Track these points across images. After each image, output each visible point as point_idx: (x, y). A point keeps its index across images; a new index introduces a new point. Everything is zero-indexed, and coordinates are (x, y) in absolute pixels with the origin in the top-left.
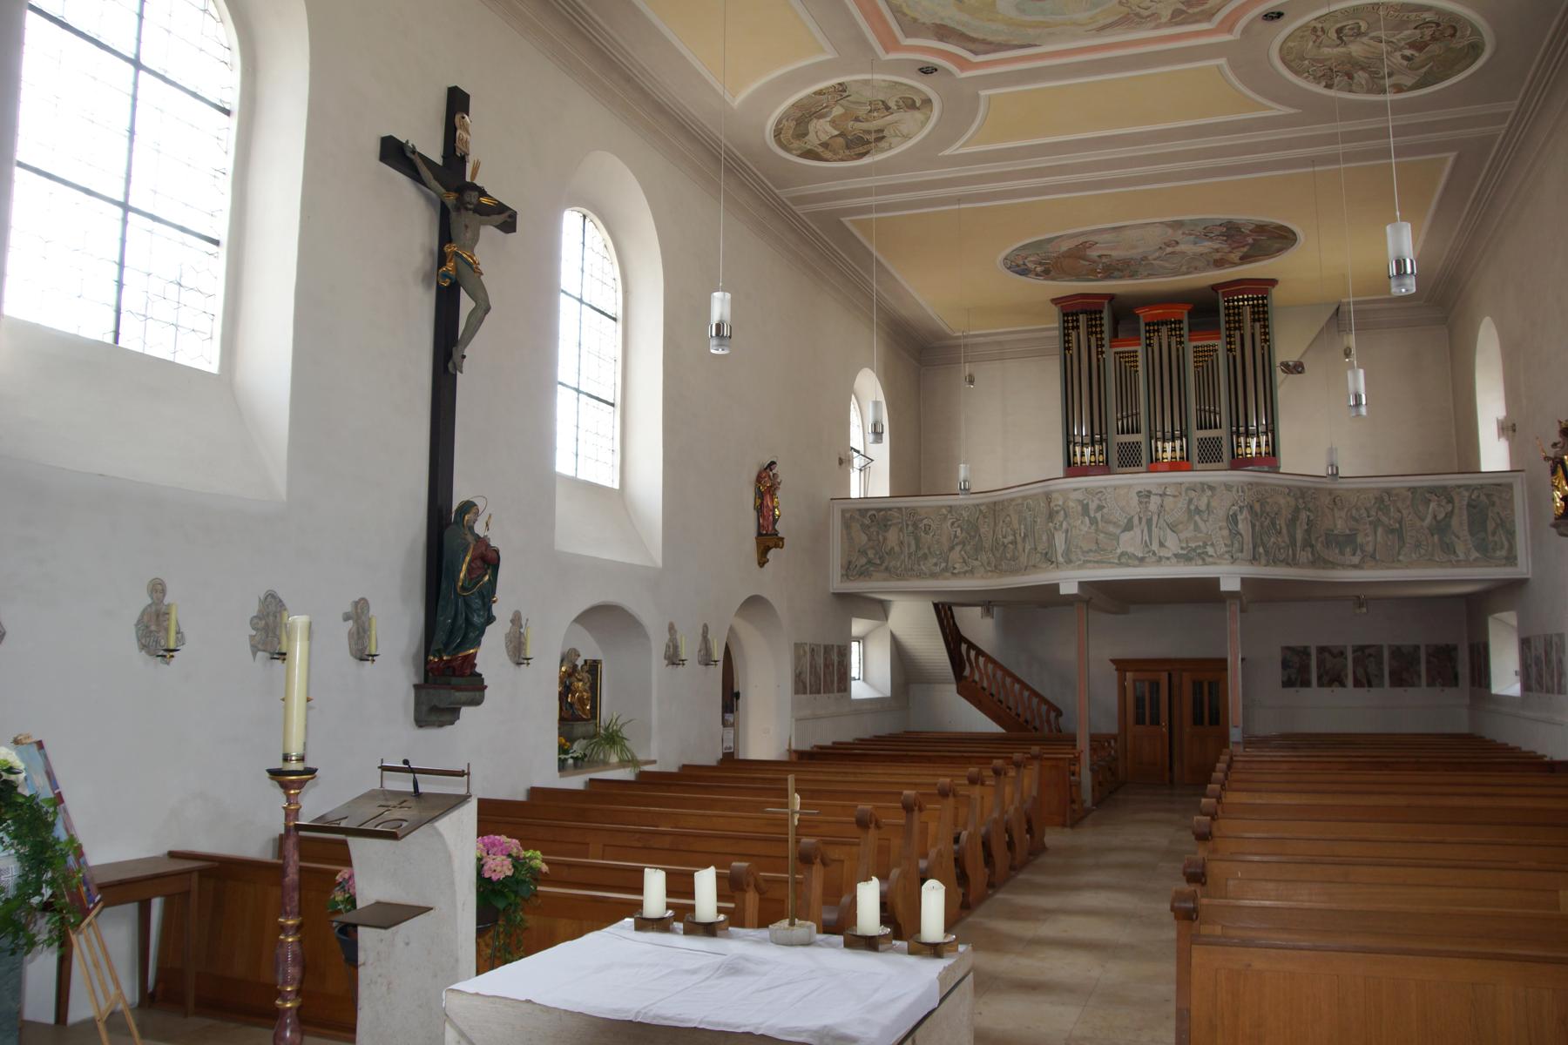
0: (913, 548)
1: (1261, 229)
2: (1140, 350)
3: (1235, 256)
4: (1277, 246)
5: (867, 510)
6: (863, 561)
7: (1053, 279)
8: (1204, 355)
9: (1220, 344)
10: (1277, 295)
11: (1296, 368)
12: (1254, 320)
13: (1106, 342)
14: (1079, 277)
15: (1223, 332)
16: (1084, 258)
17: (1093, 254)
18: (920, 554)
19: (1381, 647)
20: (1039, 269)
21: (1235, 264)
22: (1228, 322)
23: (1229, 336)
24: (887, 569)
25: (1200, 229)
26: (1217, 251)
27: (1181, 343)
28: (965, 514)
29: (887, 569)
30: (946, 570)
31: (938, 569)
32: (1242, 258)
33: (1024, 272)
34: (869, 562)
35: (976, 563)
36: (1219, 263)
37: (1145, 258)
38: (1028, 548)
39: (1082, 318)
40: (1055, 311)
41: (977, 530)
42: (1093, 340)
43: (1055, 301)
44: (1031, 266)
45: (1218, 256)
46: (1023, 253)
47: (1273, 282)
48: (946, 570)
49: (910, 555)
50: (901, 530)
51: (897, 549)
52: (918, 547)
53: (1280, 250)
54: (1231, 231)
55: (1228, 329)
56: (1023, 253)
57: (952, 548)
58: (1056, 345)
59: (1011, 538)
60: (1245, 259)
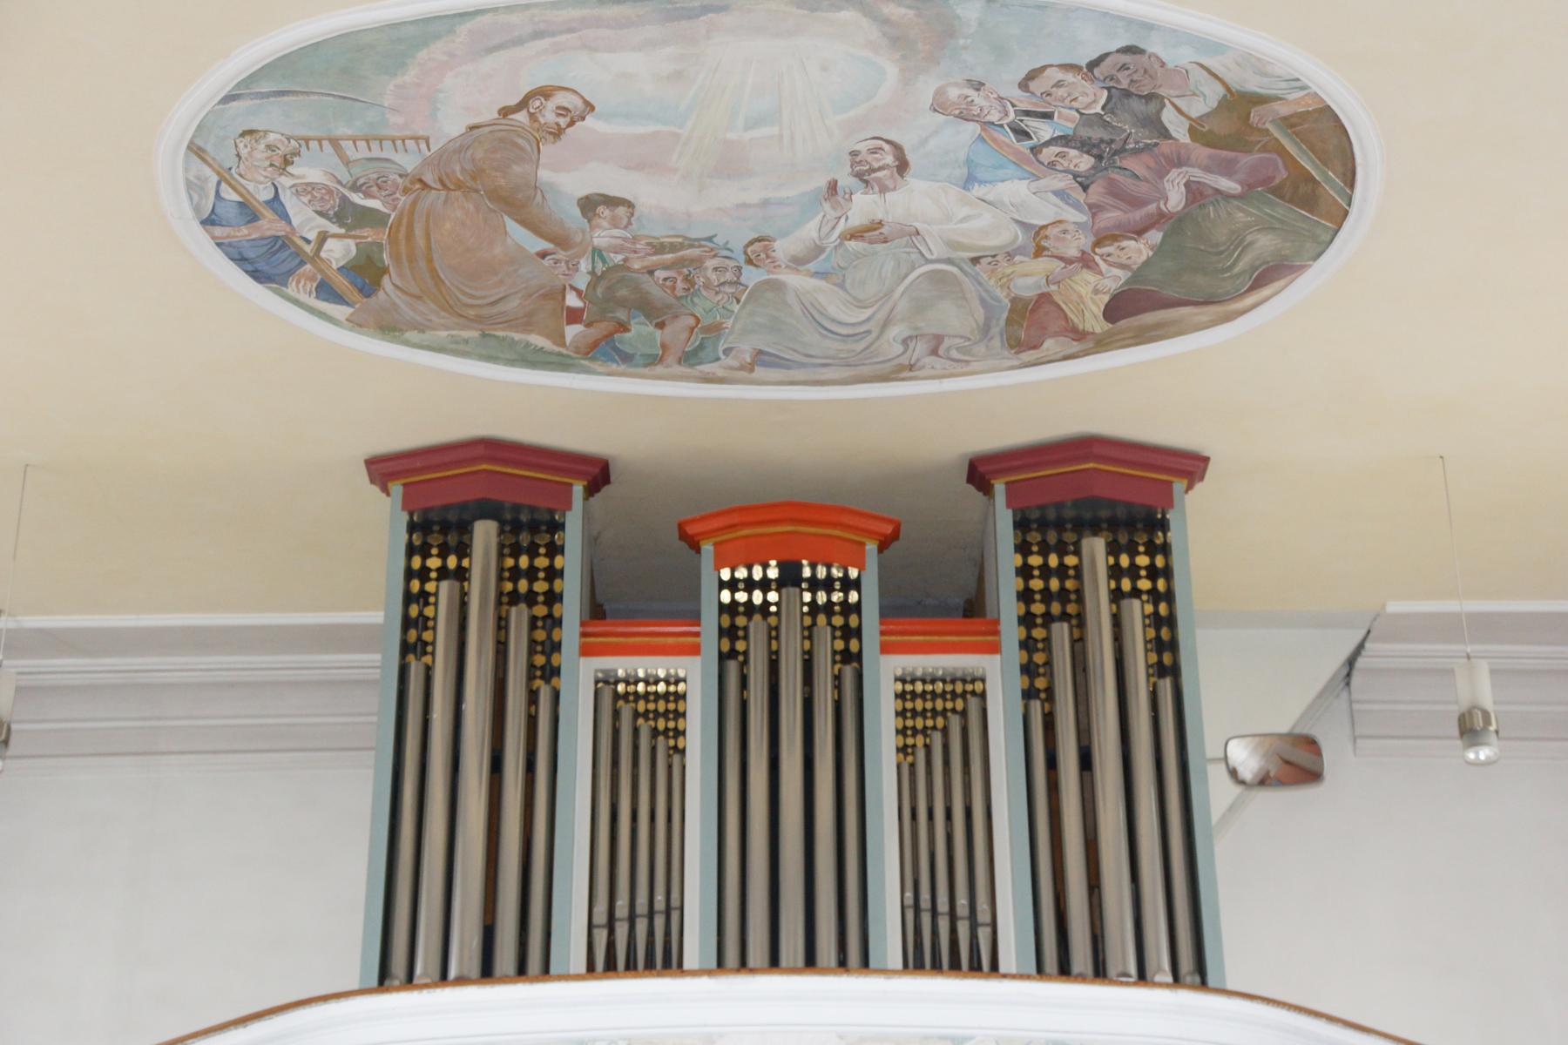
1: (1240, 117)
2: (694, 675)
3: (1088, 294)
4: (1264, 244)
7: (389, 328)
8: (940, 714)
9: (998, 673)
10: (1201, 525)
11: (1297, 763)
12: (1117, 596)
13: (570, 634)
14: (491, 329)
15: (1011, 633)
16: (519, 203)
17: (566, 178)
20: (339, 251)
21: (1086, 342)
22: (1025, 596)
23: (1027, 645)
25: (1006, 82)
26: (1038, 241)
27: (850, 657)
32: (1117, 309)
33: (270, 262)
36: (1031, 326)
37: (759, 250)
39: (485, 534)
40: (381, 521)
42: (519, 616)
43: (382, 469)
44: (305, 220)
45: (1030, 277)
46: (278, 121)
47: (1191, 466)
53: (1268, 274)
54: (1119, 118)
55: (1027, 620)
56: (278, 121)
58: (377, 664)
60: (1134, 311)
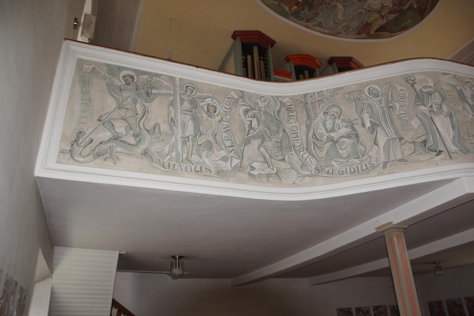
0: (190, 131)
5: (120, 69)
6: (107, 135)
18: (201, 140)
19: (386, 306)
24: (145, 153)
28: (261, 105)
29: (145, 153)
30: (240, 168)
31: (227, 166)
34: (116, 138)
35: (283, 165)
38: (382, 140)
41: (279, 123)
48: (240, 168)
49: (185, 140)
50: (172, 104)
51: (164, 127)
52: (198, 132)
57: (247, 142)
59: (344, 131)
